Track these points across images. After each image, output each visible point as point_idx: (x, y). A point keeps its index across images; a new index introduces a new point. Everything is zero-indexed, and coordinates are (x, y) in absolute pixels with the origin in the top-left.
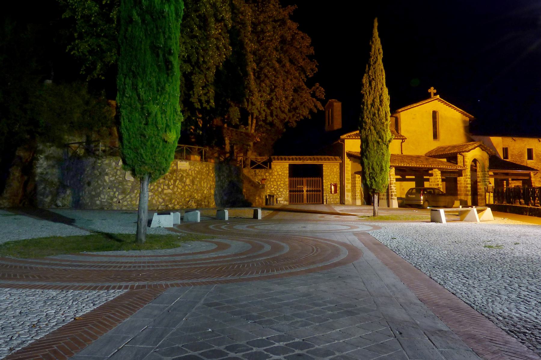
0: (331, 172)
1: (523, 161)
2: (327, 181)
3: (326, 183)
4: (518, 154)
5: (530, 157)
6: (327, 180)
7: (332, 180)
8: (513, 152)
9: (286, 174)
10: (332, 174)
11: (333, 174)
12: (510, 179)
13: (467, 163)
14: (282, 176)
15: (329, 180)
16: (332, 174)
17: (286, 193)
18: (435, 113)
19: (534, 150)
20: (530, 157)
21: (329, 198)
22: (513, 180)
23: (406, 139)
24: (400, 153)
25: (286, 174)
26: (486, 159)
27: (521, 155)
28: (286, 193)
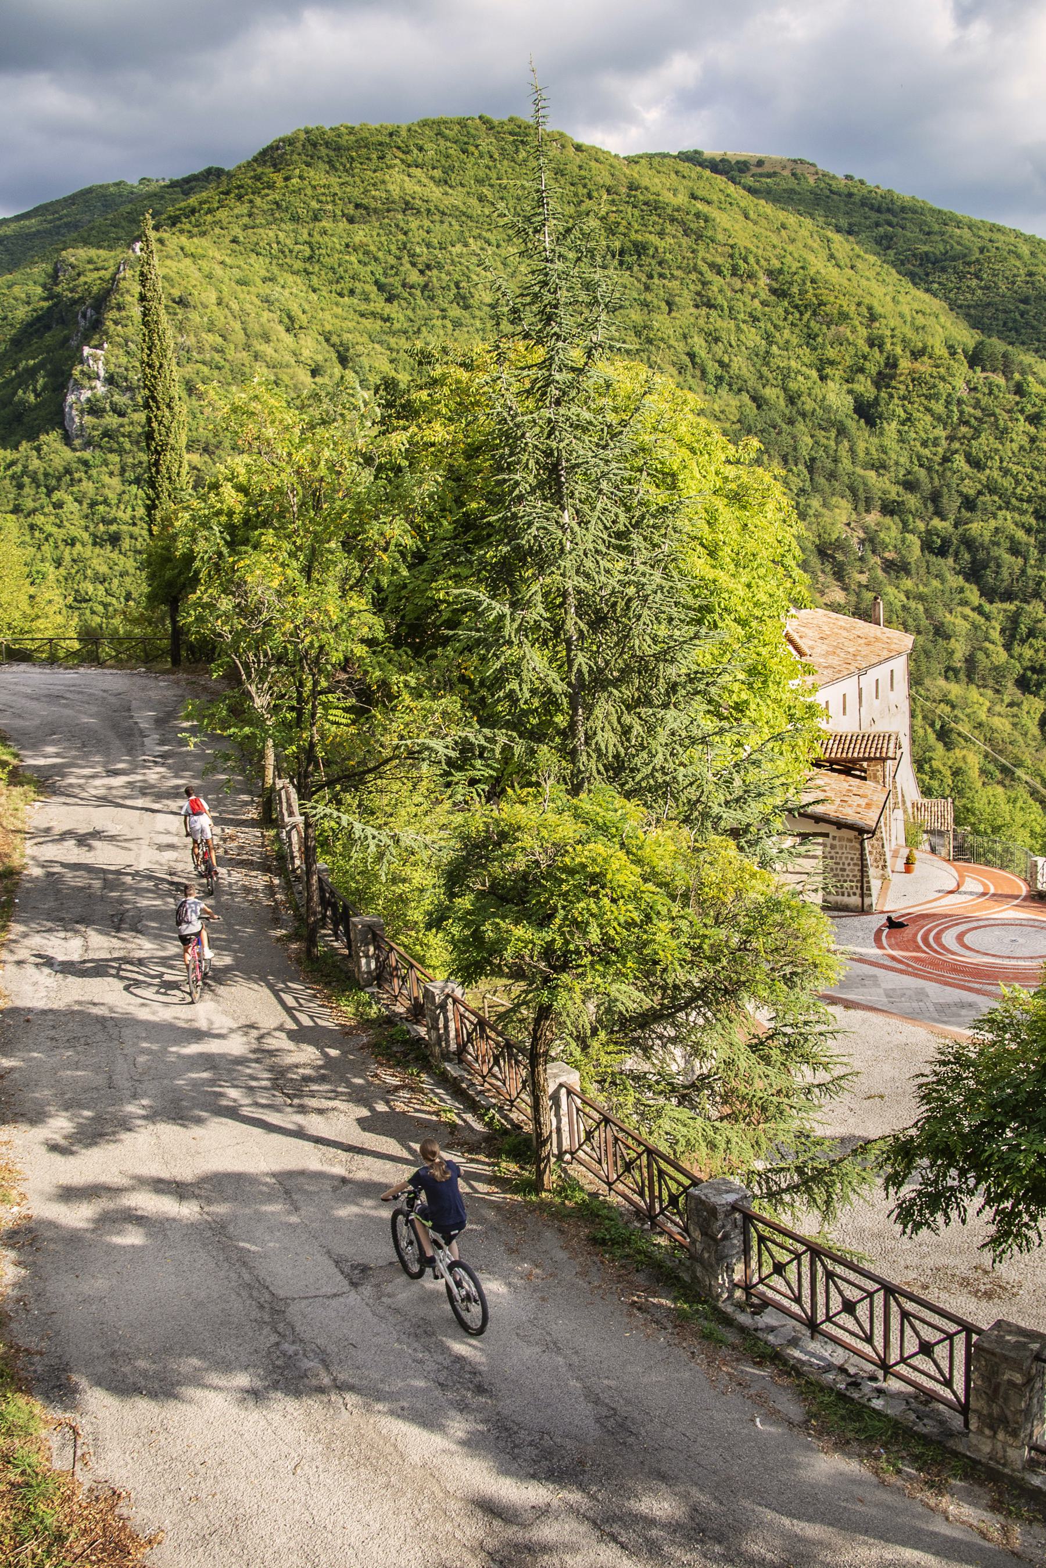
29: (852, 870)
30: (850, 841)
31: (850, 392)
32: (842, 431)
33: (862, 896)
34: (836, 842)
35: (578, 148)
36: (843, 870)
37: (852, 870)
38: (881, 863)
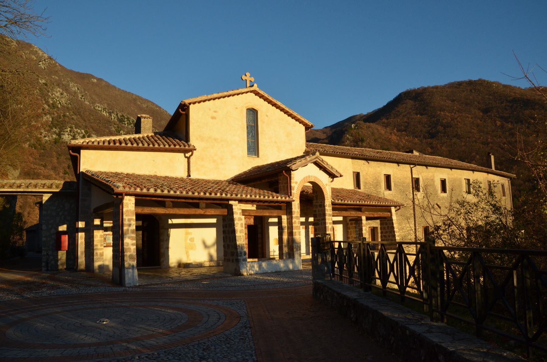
1: (380, 192)
2: (50, 226)
4: (372, 182)
5: (389, 187)
8: (366, 179)
10: (60, 214)
12: (364, 218)
13: (294, 190)
16: (60, 214)
18: (253, 113)
19: (392, 177)
20: (389, 187)
22: (368, 219)
23: (195, 150)
24: (184, 175)
26: (326, 185)
27: (377, 185)
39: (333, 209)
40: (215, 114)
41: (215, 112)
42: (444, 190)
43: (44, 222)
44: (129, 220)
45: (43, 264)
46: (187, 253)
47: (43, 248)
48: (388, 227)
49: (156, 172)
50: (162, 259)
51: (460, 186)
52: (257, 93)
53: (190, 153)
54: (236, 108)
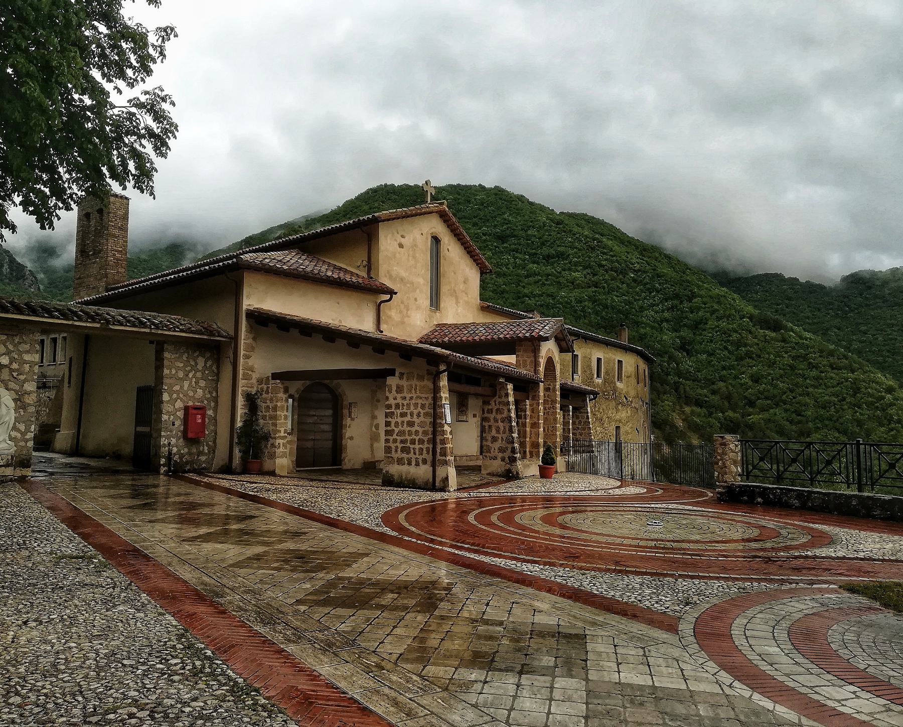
0: (188, 368)
2: (175, 396)
3: (173, 402)
6: (175, 392)
7: (191, 394)
9: (27, 367)
10: (191, 375)
11: (194, 376)
14: (11, 370)
15: (181, 395)
17: (23, 434)
21: (179, 451)
23: (396, 293)
25: (27, 367)
28: (23, 434)
29: (421, 425)
30: (421, 378)
31: (678, 337)
32: (672, 358)
33: (434, 465)
34: (404, 383)
35: (532, 204)
36: (411, 424)
37: (421, 425)
38: (508, 454)
39: (562, 396)
40: (403, 241)
41: (403, 237)
42: (598, 376)
43: (166, 388)
44: (446, 398)
45: (163, 461)
46: (372, 445)
47: (163, 434)
48: (580, 422)
49: (340, 321)
50: (343, 455)
51: (613, 369)
52: (443, 216)
53: (388, 297)
54: (422, 234)
